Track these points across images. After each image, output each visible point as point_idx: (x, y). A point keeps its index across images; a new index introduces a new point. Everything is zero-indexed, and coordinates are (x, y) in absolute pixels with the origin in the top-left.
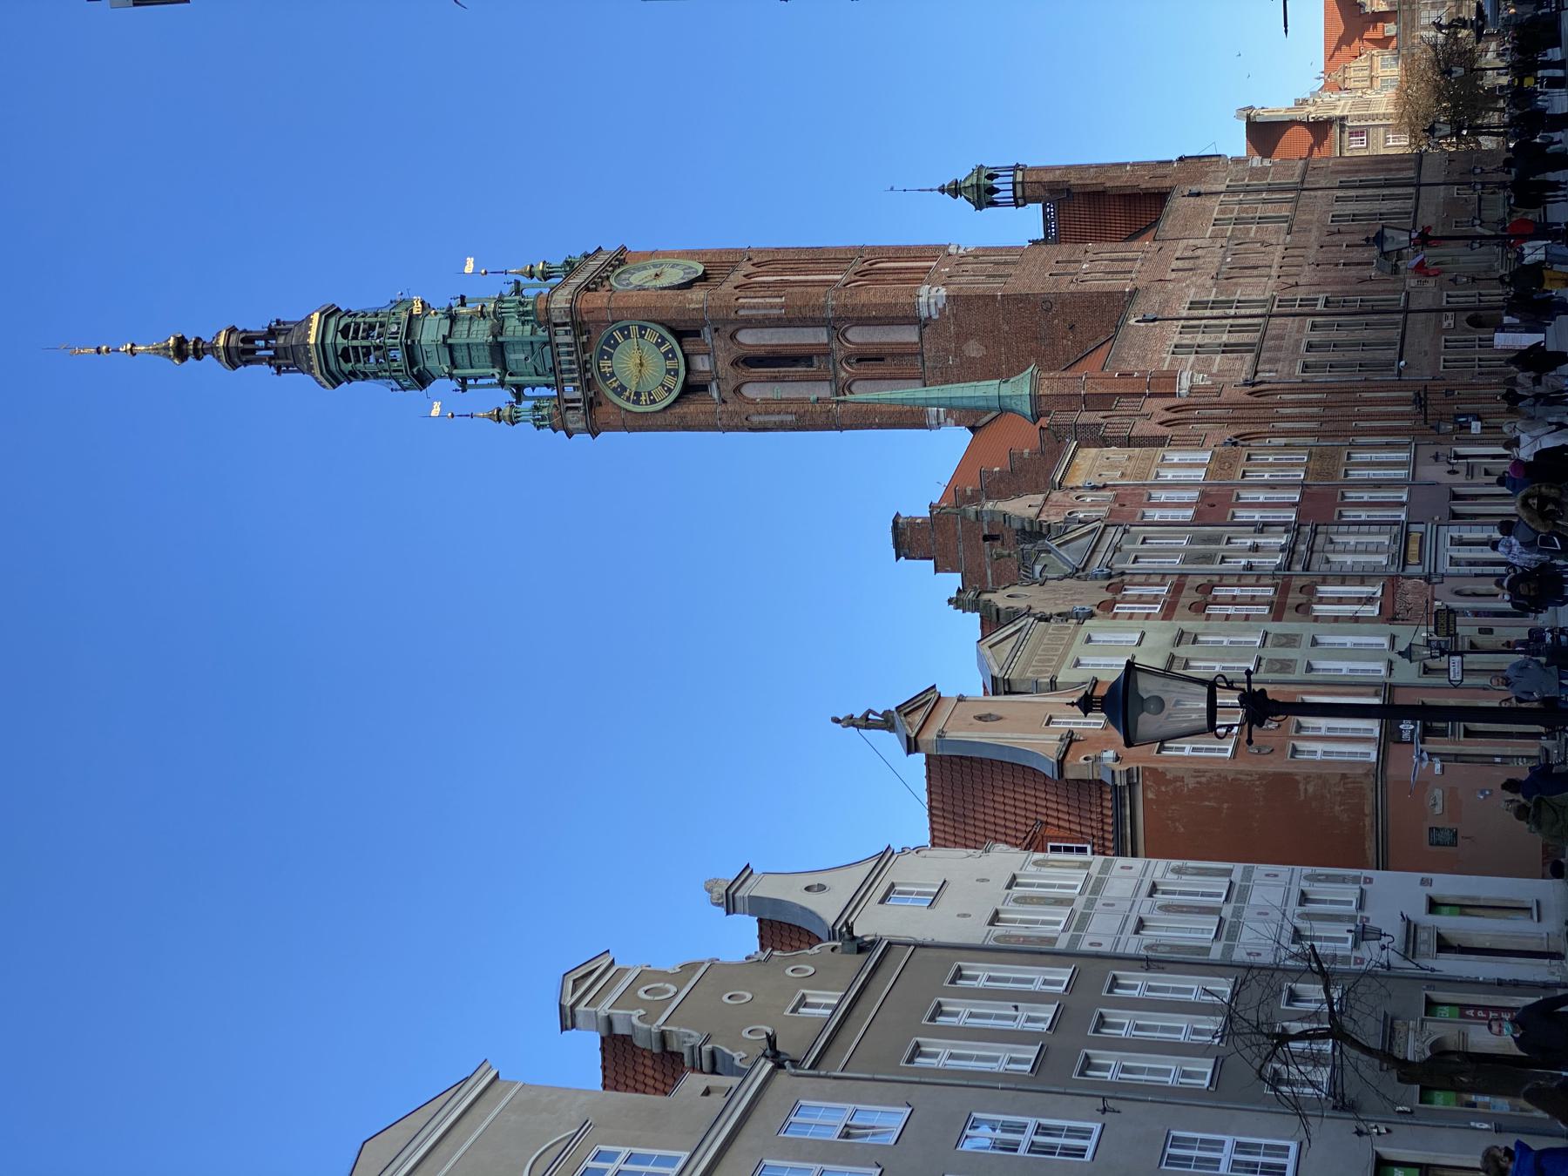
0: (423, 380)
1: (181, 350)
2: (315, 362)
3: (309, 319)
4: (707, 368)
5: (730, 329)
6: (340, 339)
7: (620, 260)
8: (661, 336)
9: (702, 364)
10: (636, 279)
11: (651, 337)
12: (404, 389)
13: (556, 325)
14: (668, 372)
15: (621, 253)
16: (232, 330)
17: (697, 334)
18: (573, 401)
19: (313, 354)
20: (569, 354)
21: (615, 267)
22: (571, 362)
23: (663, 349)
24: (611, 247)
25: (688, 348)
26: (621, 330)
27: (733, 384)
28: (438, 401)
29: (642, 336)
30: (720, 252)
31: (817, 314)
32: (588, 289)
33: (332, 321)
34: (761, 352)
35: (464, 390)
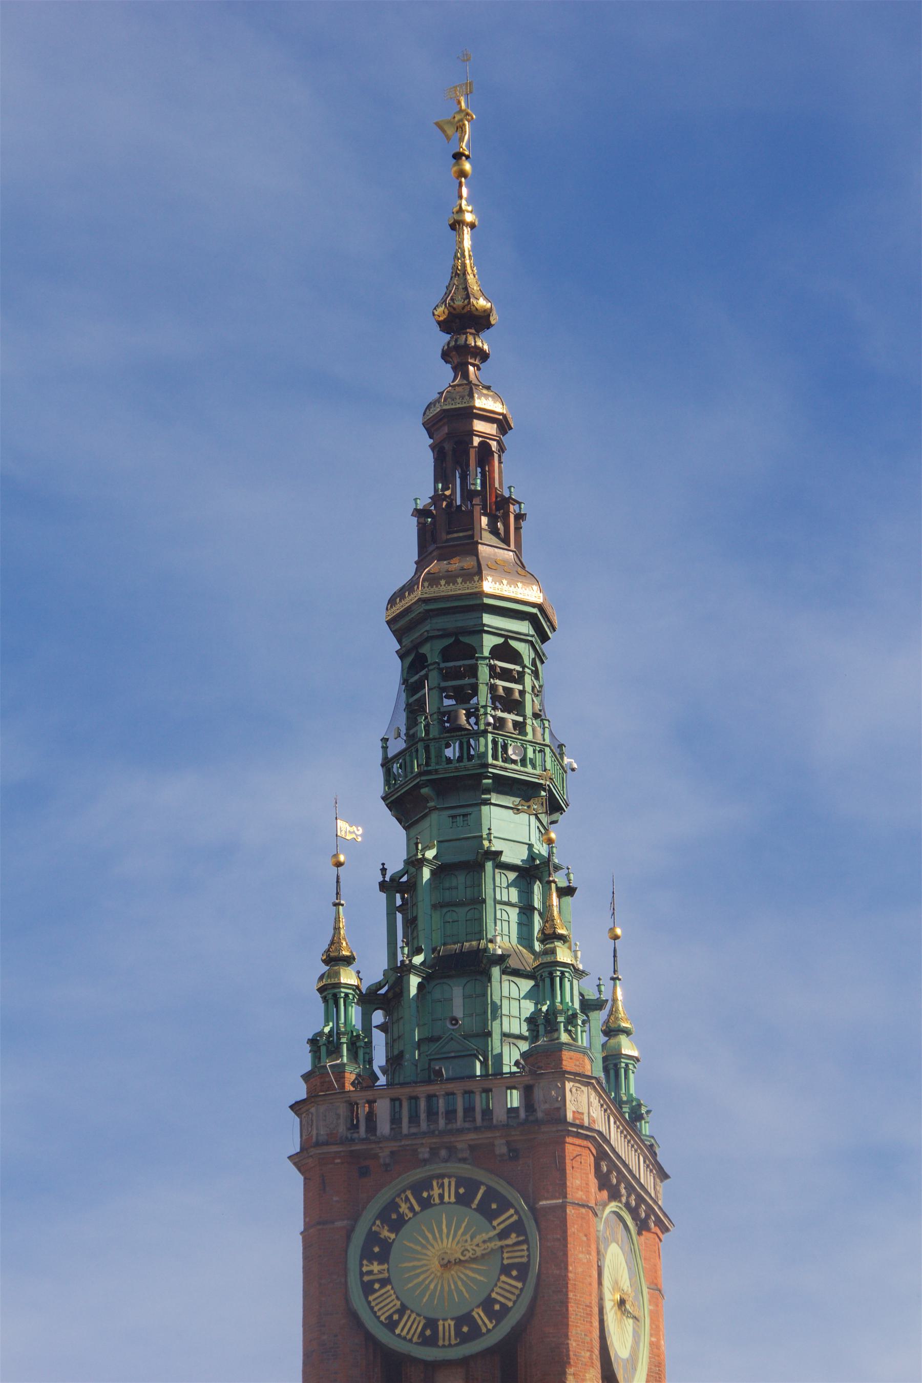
0: (404, 803)
1: (462, 321)
2: (444, 589)
3: (532, 578)
6: (489, 642)
8: (505, 1310)
10: (616, 1260)
11: (507, 1290)
12: (386, 764)
15: (659, 1222)
16: (503, 425)
19: (461, 588)
20: (469, 1110)
21: (634, 1212)
23: (479, 1315)
28: (369, 836)
29: (505, 1270)
32: (601, 1156)
33: (524, 627)
35: (383, 886)
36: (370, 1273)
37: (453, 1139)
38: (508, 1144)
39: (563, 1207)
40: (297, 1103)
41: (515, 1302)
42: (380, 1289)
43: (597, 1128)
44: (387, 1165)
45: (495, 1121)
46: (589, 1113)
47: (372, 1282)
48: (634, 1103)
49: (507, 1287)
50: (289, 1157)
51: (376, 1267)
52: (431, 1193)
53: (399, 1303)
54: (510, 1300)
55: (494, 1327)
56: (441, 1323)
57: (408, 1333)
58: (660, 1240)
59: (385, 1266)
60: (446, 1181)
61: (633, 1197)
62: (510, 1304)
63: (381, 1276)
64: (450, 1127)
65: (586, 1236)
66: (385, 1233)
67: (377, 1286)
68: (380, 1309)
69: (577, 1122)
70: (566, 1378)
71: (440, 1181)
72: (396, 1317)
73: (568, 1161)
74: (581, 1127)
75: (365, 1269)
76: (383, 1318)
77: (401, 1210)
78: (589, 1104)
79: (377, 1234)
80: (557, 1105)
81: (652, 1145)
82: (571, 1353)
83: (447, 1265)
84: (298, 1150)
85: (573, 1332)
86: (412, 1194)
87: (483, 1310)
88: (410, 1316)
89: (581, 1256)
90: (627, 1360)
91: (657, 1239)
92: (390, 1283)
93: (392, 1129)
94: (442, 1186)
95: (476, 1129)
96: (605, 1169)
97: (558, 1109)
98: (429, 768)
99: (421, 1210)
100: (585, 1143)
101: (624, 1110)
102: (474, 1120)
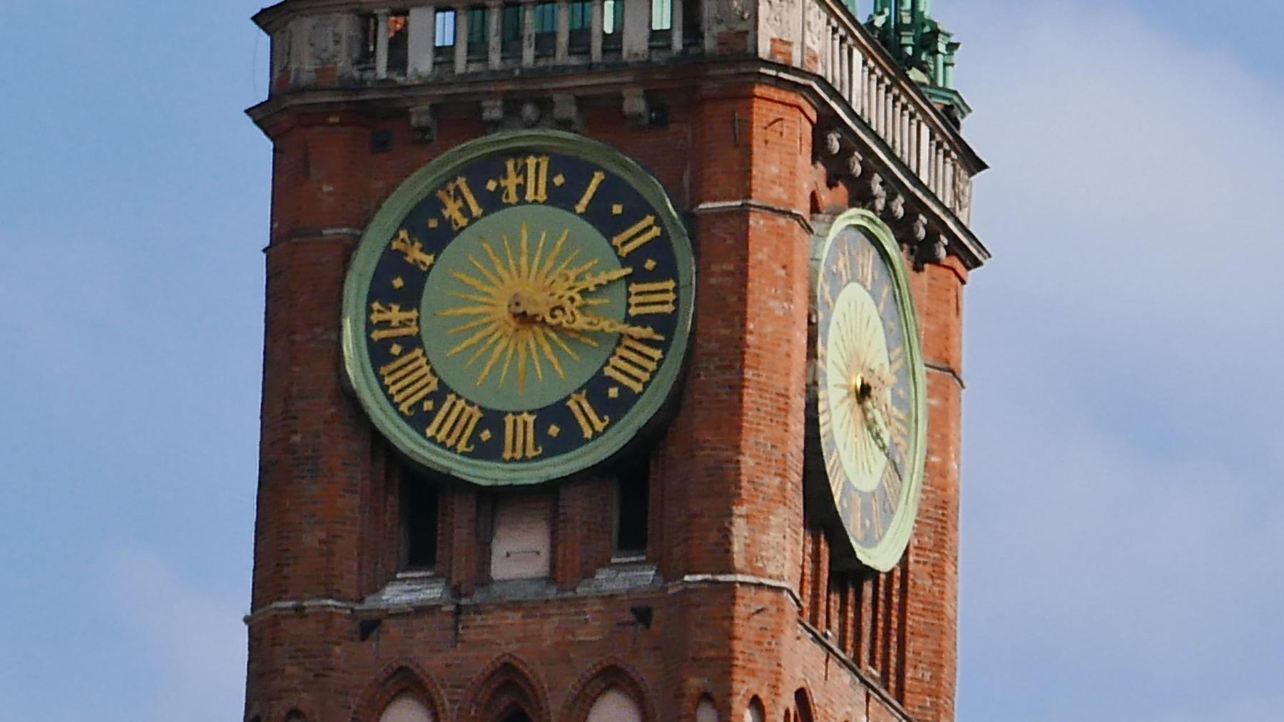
4: (500, 569)
5: (645, 668)
7: (930, 242)
8: (629, 399)
9: (519, 555)
14: (492, 419)
15: (956, 248)
17: (633, 536)
18: (399, 42)
21: (903, 230)
22: (545, 41)
24: (981, 208)
25: (576, 505)
26: (660, 247)
27: (432, 664)
30: (940, 627)
32: (825, 123)
36: (385, 324)
37: (545, 86)
38: (648, 96)
39: (743, 213)
40: (263, 11)
41: (646, 385)
42: (401, 355)
43: (820, 72)
44: (424, 130)
45: (625, 54)
46: (803, 43)
47: (387, 342)
48: (927, 29)
50: (248, 111)
51: (395, 314)
52: (503, 183)
53: (435, 381)
54: (637, 380)
55: (606, 429)
56: (509, 419)
57: (449, 435)
58: (963, 282)
59: (413, 314)
60: (531, 161)
61: (900, 199)
62: (638, 388)
63: (404, 331)
64: (541, 63)
65: (784, 267)
66: (416, 254)
67: (396, 349)
68: (400, 391)
69: (779, 59)
70: (731, 523)
71: (520, 162)
72: (428, 405)
73: (757, 131)
74: (786, 68)
75: (375, 318)
76: (404, 407)
77: (446, 214)
78: (806, 24)
79: (400, 254)
80: (742, 27)
81: (948, 109)
82: (744, 478)
83: (525, 319)
84: (265, 97)
85: (748, 441)
87: (587, 397)
88: (454, 404)
89: (773, 304)
90: (873, 493)
91: (955, 280)
92: (421, 345)
93: (435, 64)
94: (523, 171)
95: (590, 68)
96: (835, 146)
99: (484, 215)
100: (792, 97)
101: (904, 41)
102: (588, 52)
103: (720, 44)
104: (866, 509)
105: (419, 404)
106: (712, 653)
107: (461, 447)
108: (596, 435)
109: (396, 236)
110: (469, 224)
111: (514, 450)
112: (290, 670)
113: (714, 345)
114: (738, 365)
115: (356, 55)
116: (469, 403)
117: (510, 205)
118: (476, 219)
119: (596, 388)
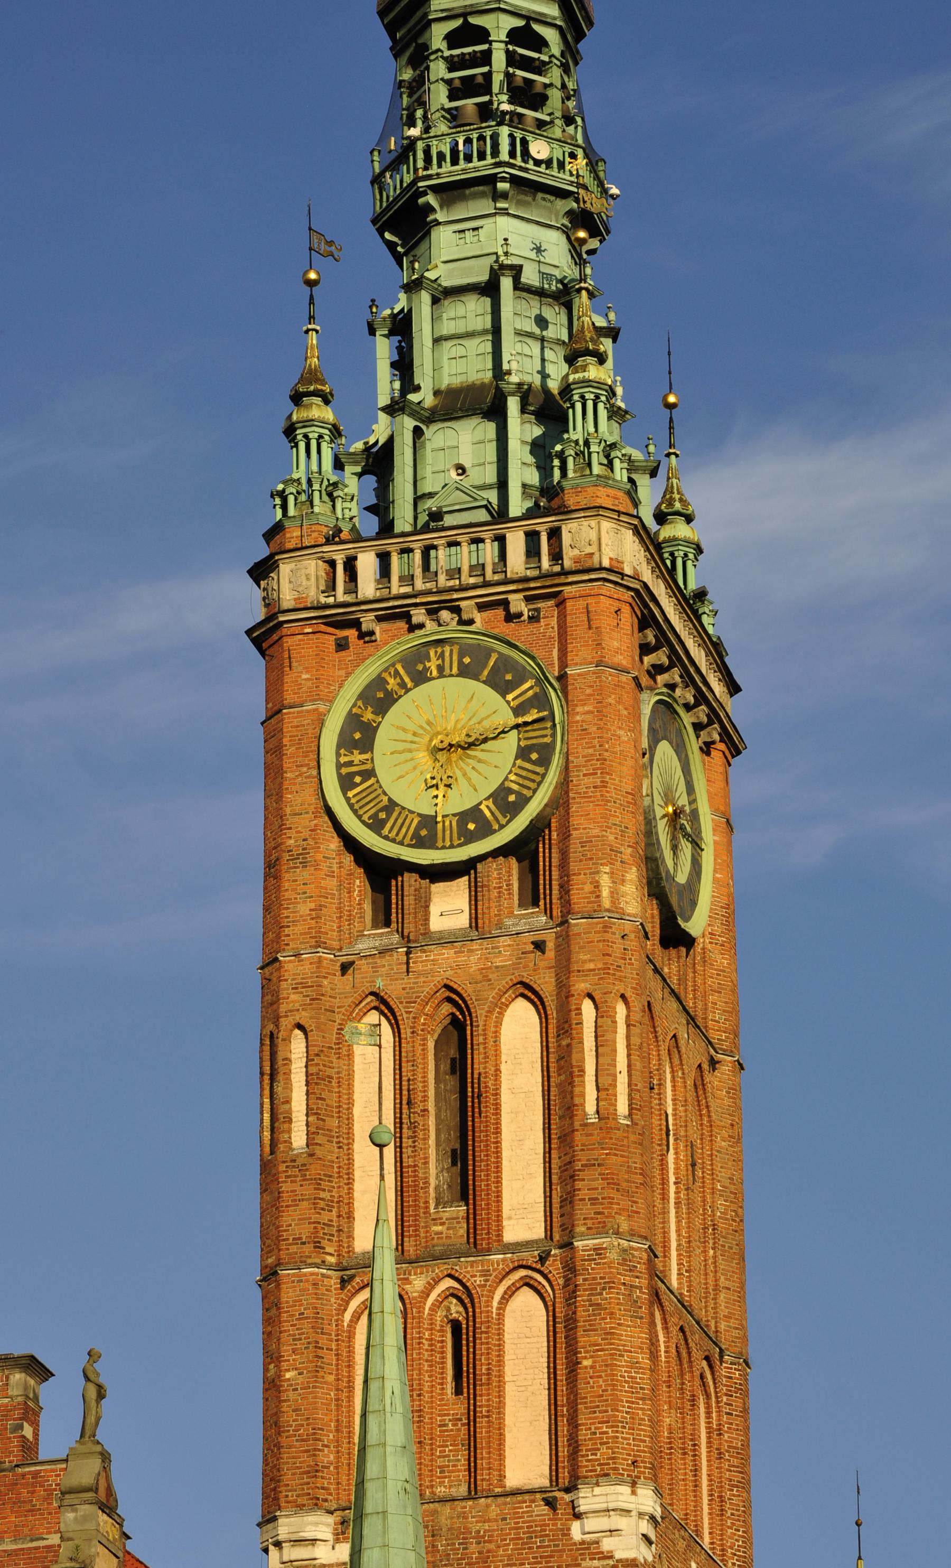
4: (436, 924)
13: (555, 534)
27: (393, 990)
31: (583, 1210)
34: (478, 1064)
36: (350, 764)
47: (352, 775)
49: (524, 773)
51: (357, 757)
52: (428, 665)
53: (385, 799)
57: (397, 834)
58: (730, 765)
67: (358, 779)
68: (361, 808)
71: (439, 650)
72: (383, 815)
74: (623, 575)
75: (343, 760)
77: (389, 687)
79: (358, 716)
80: (589, 550)
86: (403, 667)
92: (375, 776)
94: (442, 656)
95: (486, 584)
97: (591, 555)
98: (429, 172)
99: (415, 686)
103: (575, 562)
104: (680, 894)
105: (376, 814)
106: (592, 966)
107: (407, 841)
108: (502, 827)
109: (354, 705)
110: (405, 693)
111: (444, 841)
112: (292, 997)
113: (582, 760)
114: (599, 772)
115: (322, 588)
116: (412, 812)
117: (434, 679)
118: (411, 689)
119: (500, 795)
